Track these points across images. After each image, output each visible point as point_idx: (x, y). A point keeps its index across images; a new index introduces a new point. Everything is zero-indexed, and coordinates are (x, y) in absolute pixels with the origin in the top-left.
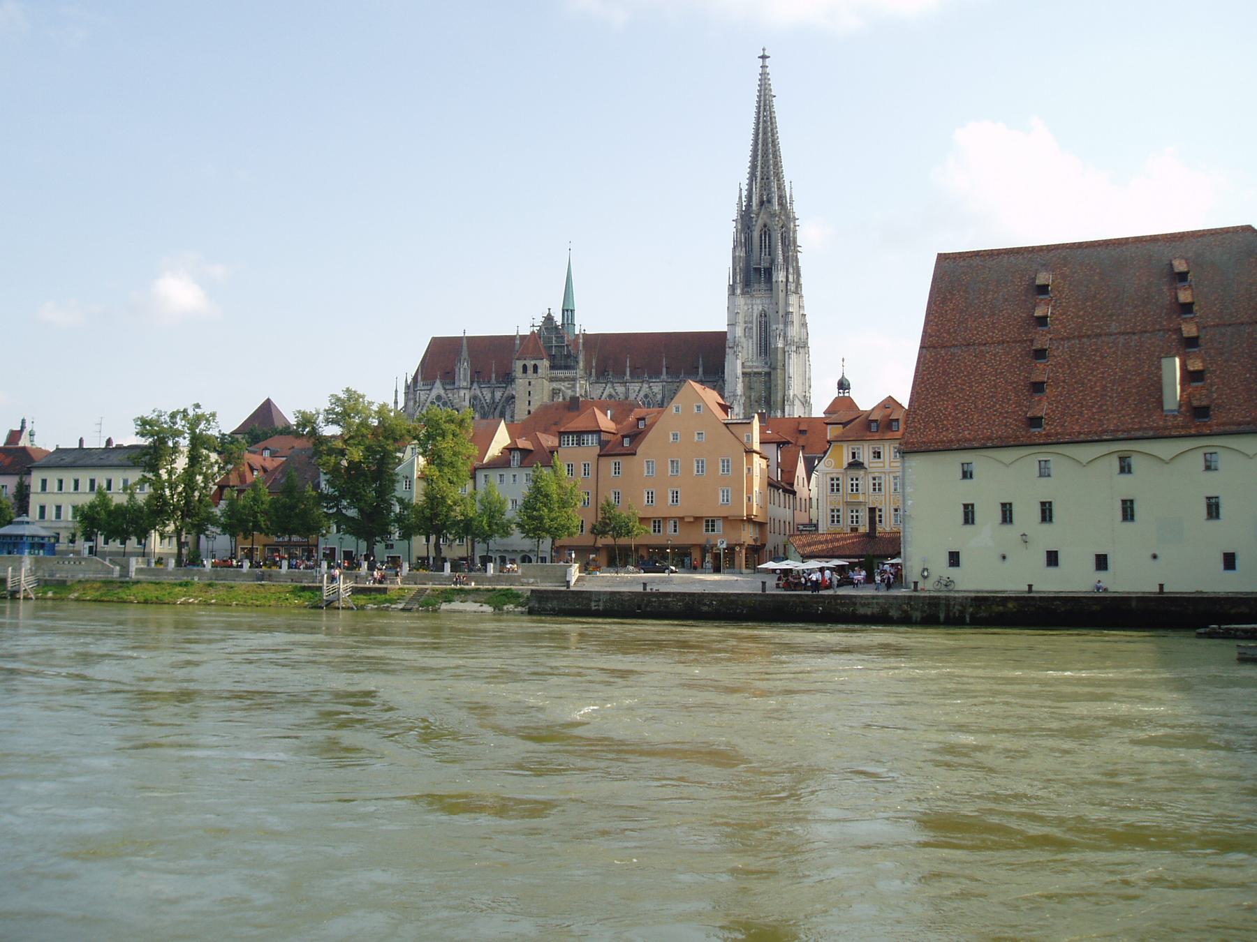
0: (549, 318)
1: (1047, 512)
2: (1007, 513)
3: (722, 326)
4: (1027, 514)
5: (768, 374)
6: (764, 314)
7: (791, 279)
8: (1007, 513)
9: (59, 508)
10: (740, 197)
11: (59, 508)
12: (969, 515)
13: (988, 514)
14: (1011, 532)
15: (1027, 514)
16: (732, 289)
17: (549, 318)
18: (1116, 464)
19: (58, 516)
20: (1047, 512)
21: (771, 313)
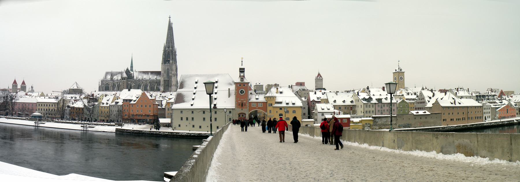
0: (127, 69)
1: (193, 119)
2: (187, 119)
3: (160, 70)
4: (190, 119)
5: (169, 80)
6: (168, 69)
7: (173, 62)
8: (187, 119)
9: (42, 109)
10: (164, 46)
11: (42, 109)
12: (182, 119)
13: (184, 119)
14: (188, 122)
15: (190, 119)
16: (162, 64)
17: (127, 69)
18: (203, 112)
19: (41, 110)
20: (193, 119)
21: (169, 69)
